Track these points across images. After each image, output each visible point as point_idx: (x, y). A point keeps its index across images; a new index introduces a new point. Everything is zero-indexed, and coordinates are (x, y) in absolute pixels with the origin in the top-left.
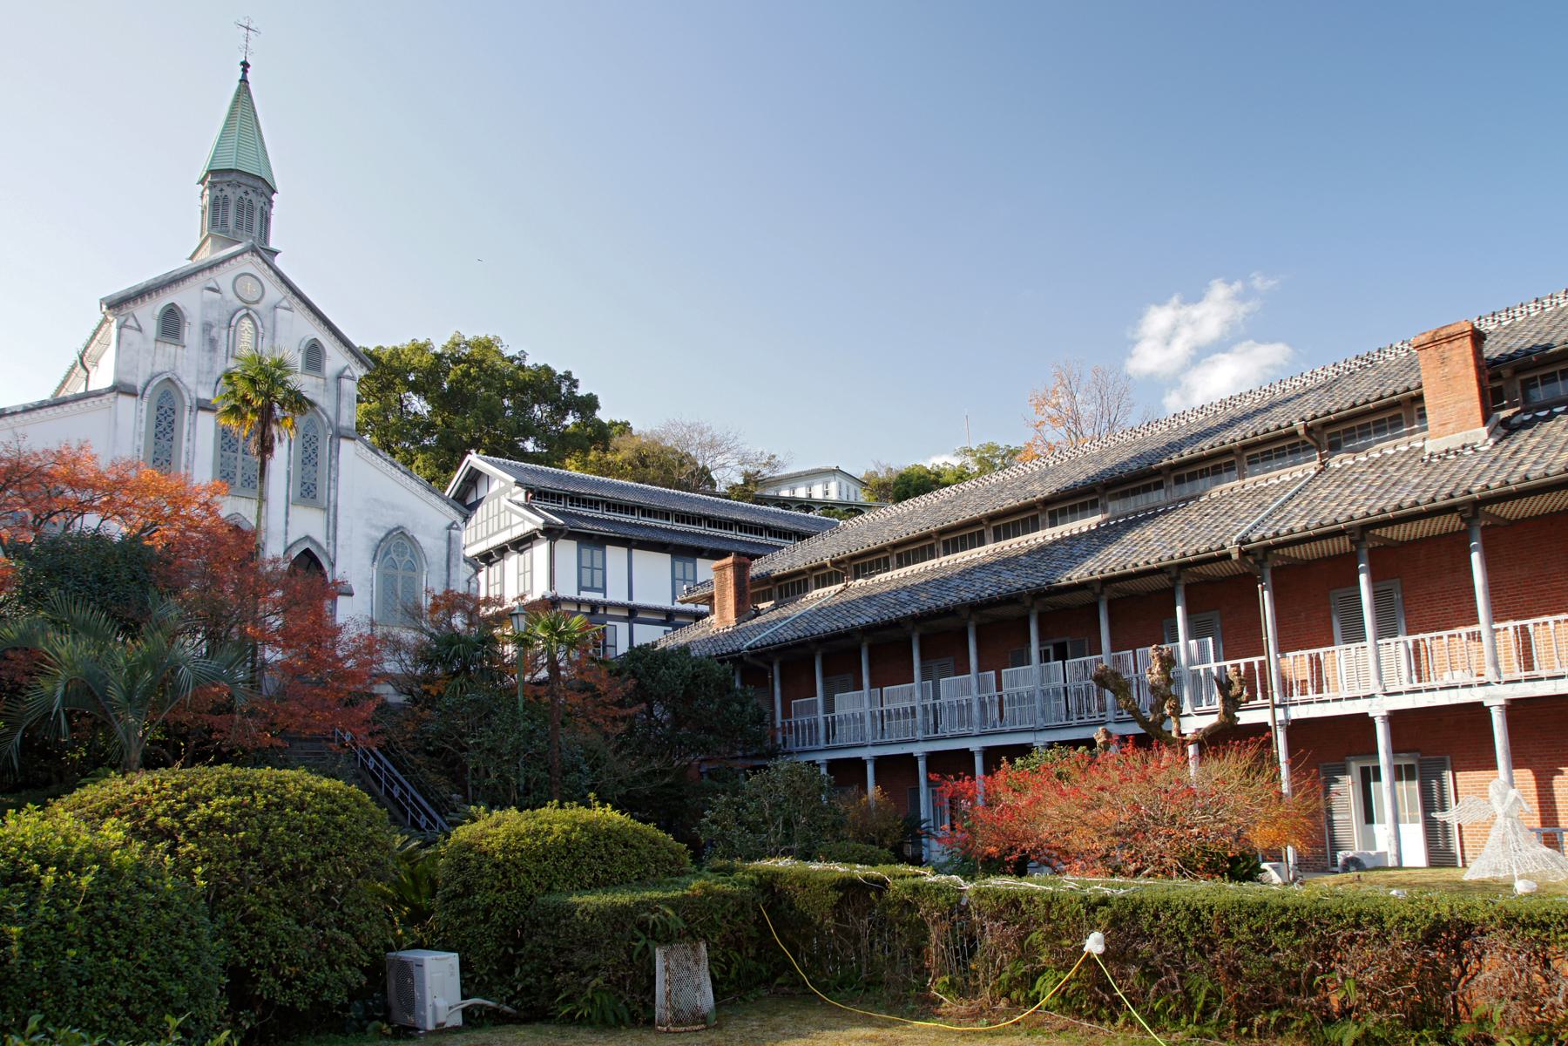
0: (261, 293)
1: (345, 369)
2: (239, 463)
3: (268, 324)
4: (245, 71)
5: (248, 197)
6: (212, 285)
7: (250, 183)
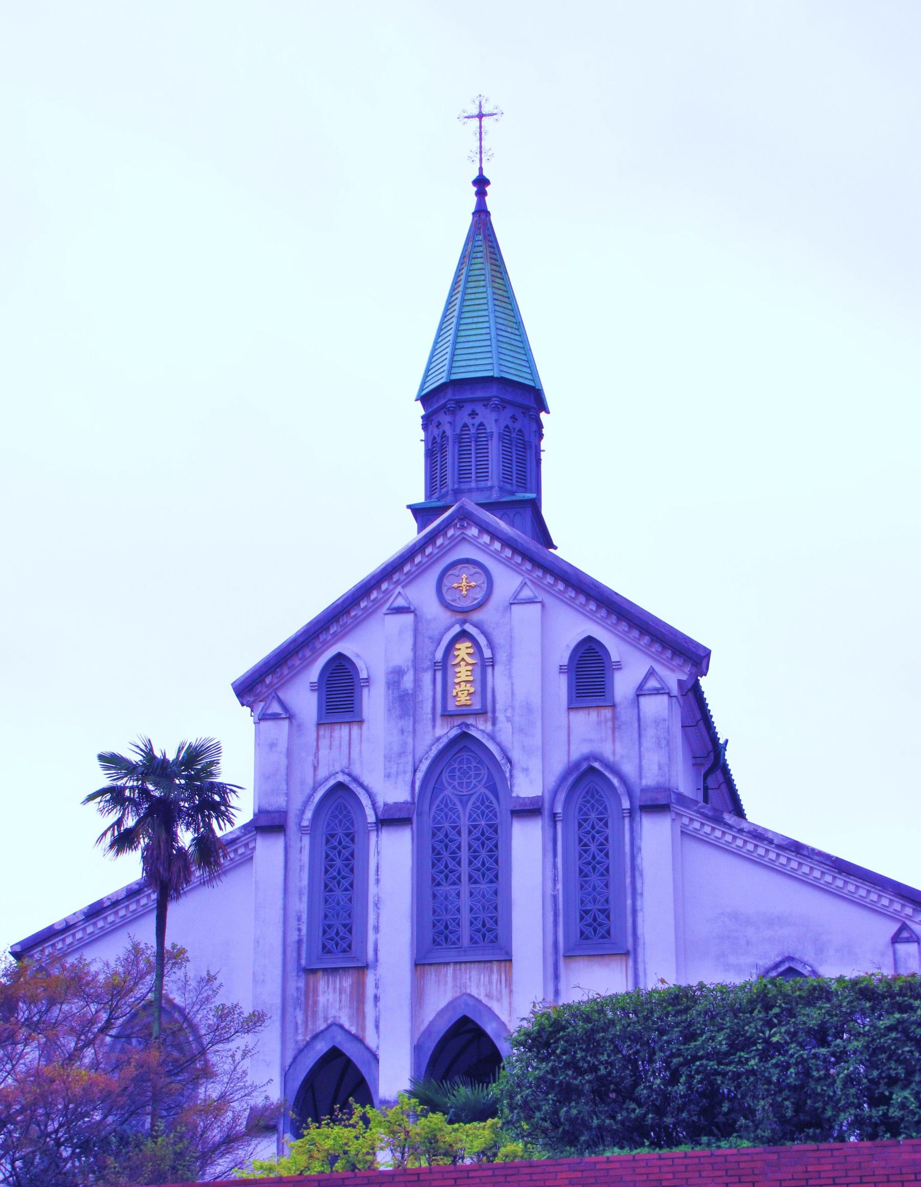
0: (485, 586)
1: (646, 679)
2: (465, 902)
3: (499, 638)
4: (481, 194)
5: (477, 421)
6: (400, 602)
7: (479, 394)
